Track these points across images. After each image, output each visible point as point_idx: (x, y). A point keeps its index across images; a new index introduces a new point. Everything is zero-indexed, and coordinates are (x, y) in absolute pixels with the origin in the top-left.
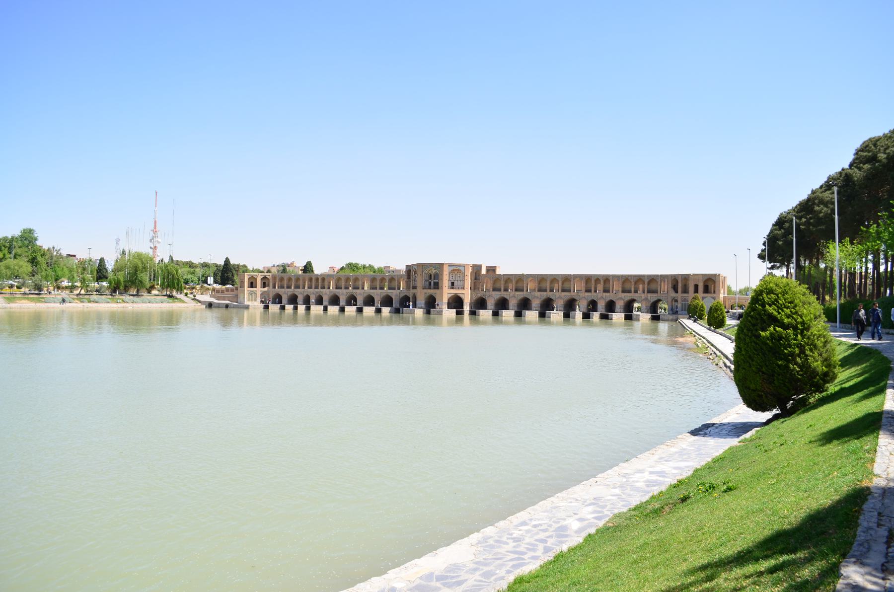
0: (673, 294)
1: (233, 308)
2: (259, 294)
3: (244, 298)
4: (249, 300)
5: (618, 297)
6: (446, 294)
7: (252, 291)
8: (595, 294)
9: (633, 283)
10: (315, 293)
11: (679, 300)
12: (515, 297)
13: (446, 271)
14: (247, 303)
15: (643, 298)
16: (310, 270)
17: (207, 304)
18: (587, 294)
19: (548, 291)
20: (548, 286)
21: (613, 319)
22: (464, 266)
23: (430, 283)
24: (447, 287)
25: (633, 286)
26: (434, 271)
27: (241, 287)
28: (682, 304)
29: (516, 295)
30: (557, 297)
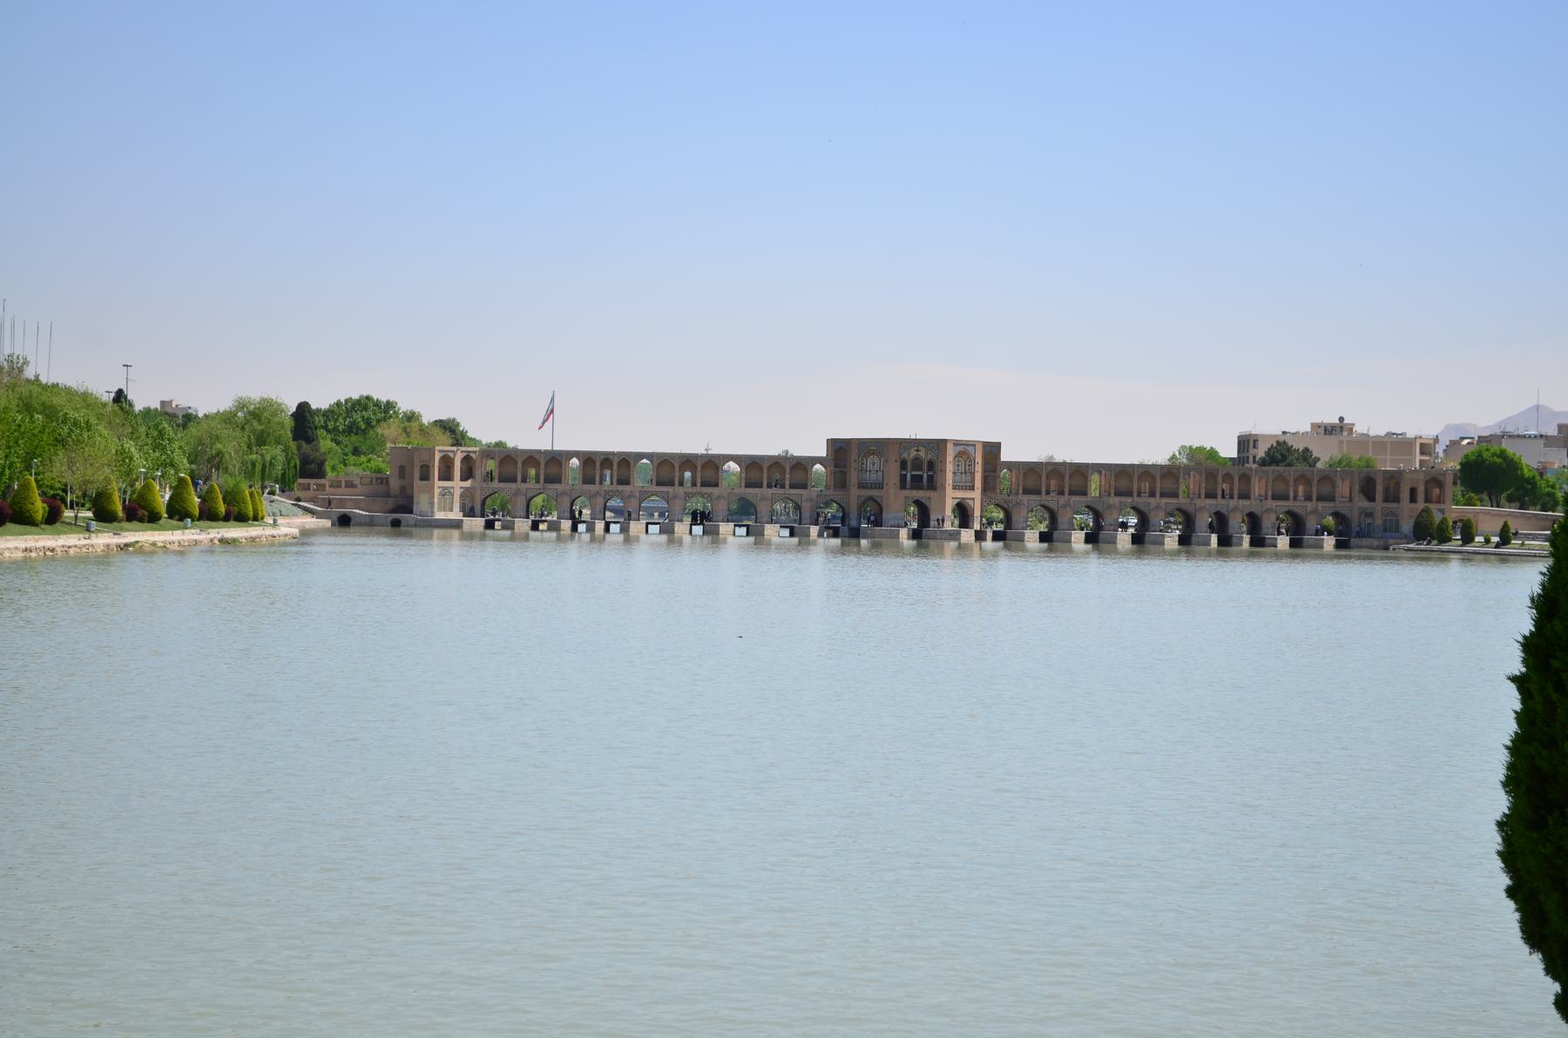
0: (1365, 504)
1: (416, 526)
2: (457, 494)
3: (432, 504)
4: (439, 510)
5: (1264, 509)
6: (951, 497)
7: (445, 488)
8: (1223, 502)
9: (1292, 483)
10: (603, 493)
11: (1378, 513)
12: (1069, 505)
13: (951, 452)
14: (439, 515)
15: (1309, 509)
16: (312, 426)
17: (335, 518)
18: (1209, 501)
19: (1135, 495)
20: (1135, 487)
21: (1278, 545)
22: (973, 444)
23: (905, 475)
24: (951, 486)
25: (1292, 489)
26: (913, 454)
27: (422, 479)
28: (1385, 521)
29: (1072, 504)
30: (1152, 507)
